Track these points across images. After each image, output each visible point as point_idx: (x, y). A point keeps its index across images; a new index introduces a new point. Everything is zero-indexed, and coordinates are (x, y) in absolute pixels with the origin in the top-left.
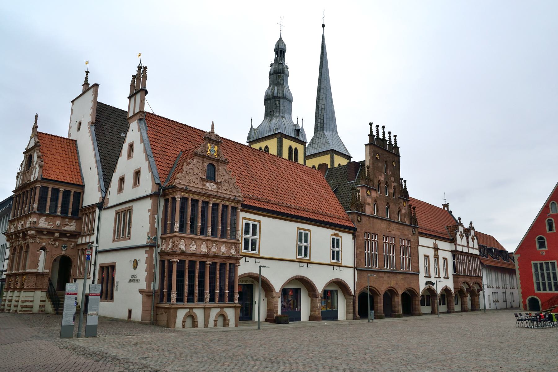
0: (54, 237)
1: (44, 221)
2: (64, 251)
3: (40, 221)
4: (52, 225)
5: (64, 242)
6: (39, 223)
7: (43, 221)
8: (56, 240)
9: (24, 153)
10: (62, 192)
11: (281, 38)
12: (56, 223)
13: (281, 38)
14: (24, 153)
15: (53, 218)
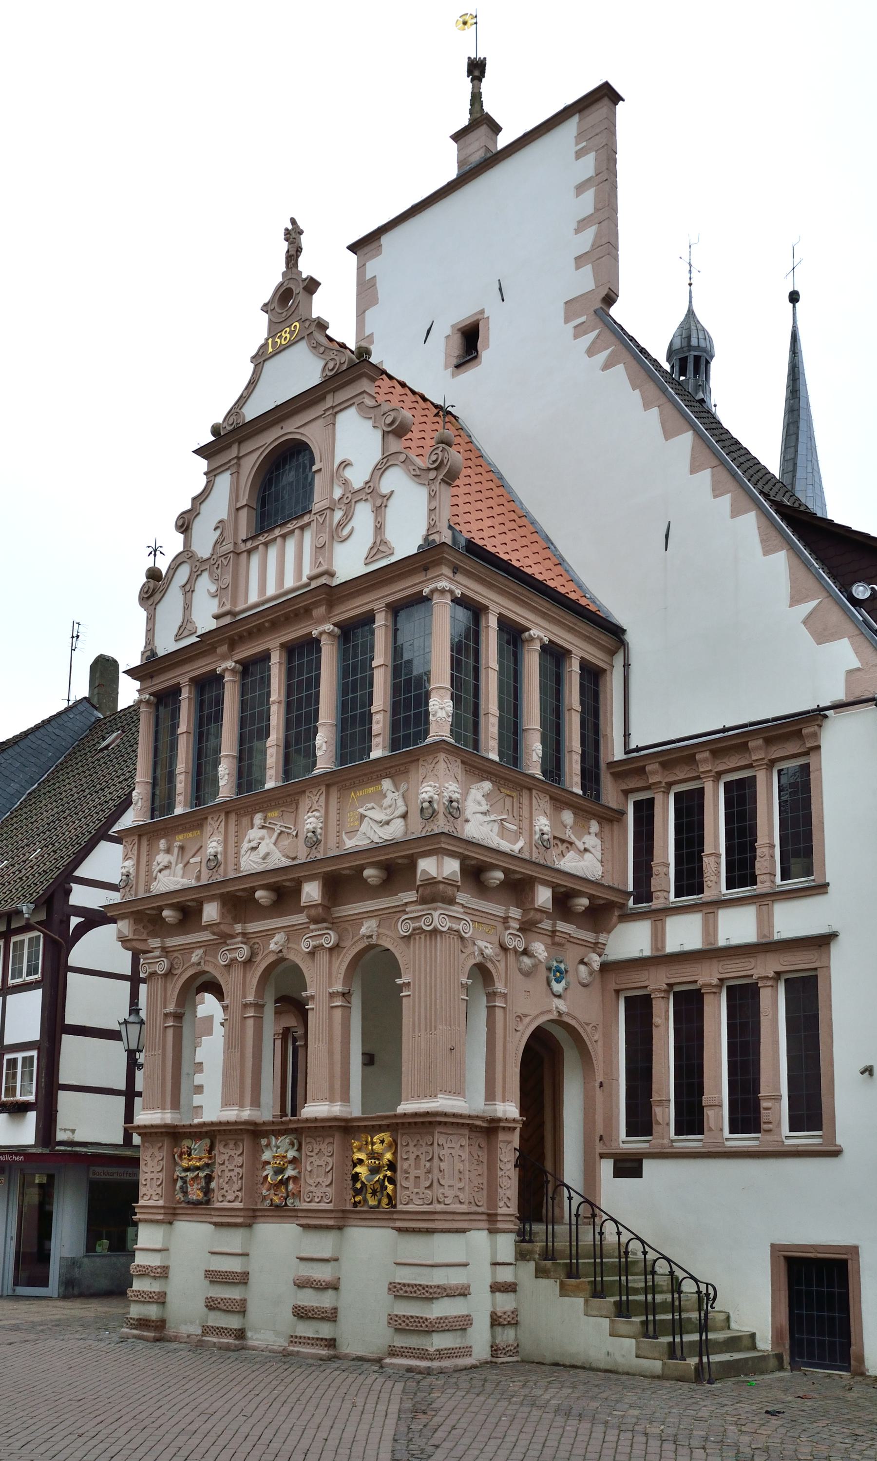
0: (525, 911)
1: (485, 808)
2: (559, 996)
3: (470, 798)
4: (519, 833)
5: (554, 944)
6: (468, 814)
7: (479, 803)
8: (527, 928)
9: (201, 452)
10: (537, 646)
11: (691, 313)
12: (531, 825)
13: (691, 313)
14: (201, 452)
15: (514, 794)
